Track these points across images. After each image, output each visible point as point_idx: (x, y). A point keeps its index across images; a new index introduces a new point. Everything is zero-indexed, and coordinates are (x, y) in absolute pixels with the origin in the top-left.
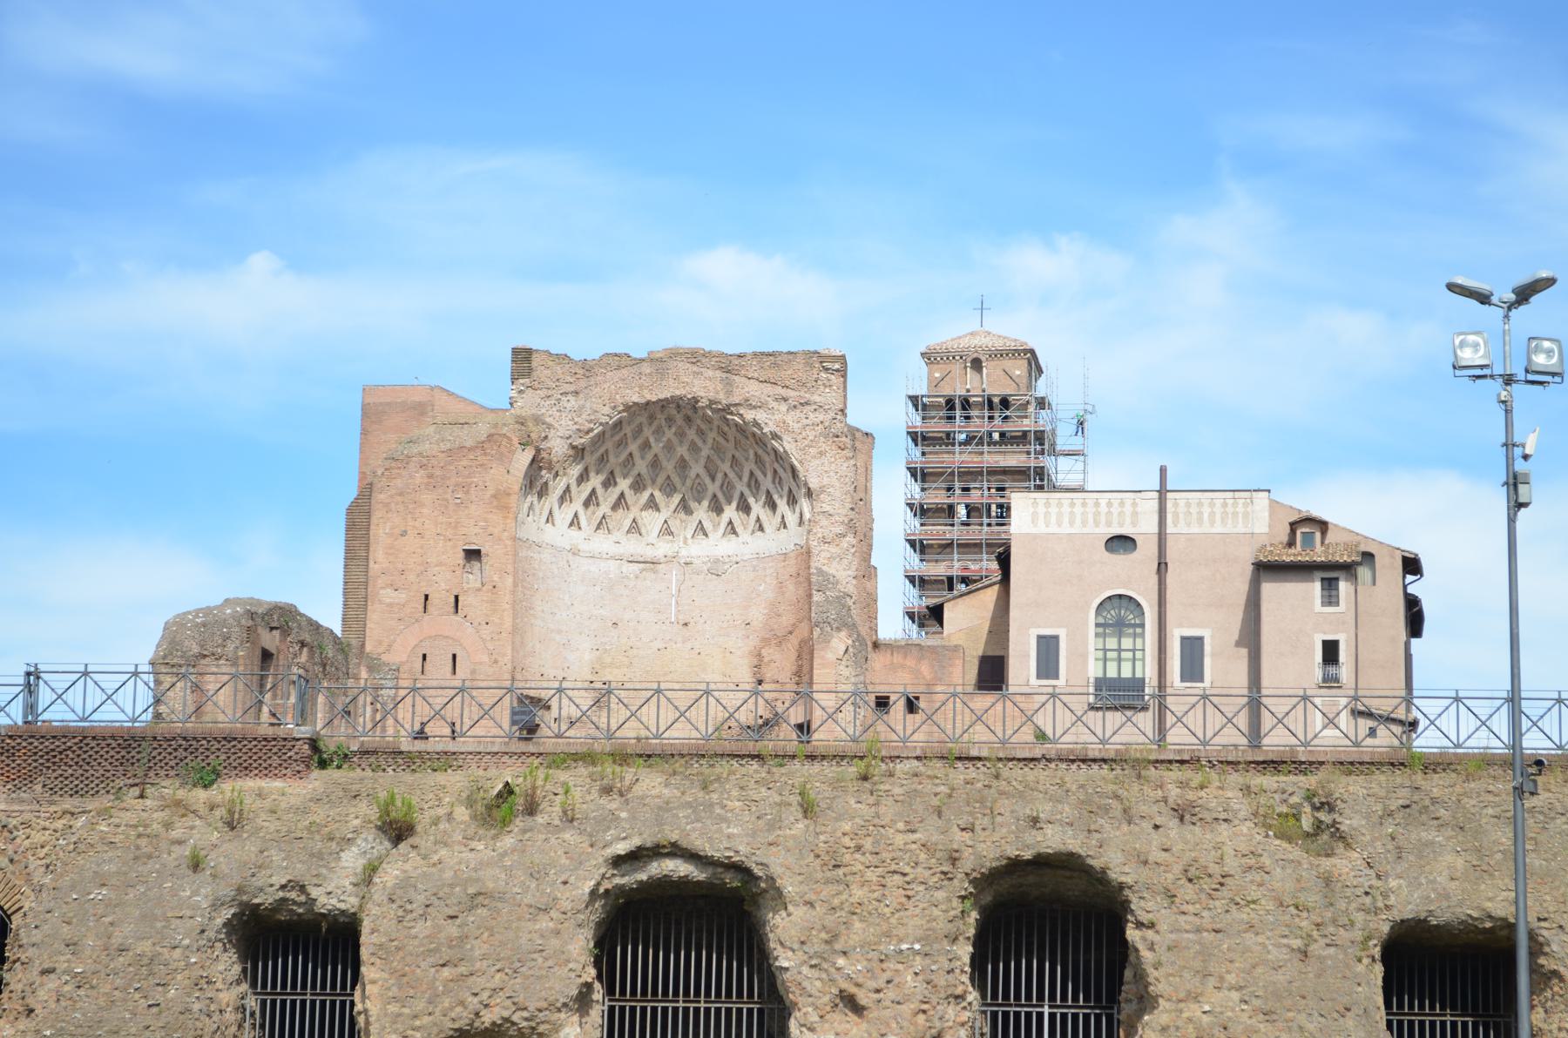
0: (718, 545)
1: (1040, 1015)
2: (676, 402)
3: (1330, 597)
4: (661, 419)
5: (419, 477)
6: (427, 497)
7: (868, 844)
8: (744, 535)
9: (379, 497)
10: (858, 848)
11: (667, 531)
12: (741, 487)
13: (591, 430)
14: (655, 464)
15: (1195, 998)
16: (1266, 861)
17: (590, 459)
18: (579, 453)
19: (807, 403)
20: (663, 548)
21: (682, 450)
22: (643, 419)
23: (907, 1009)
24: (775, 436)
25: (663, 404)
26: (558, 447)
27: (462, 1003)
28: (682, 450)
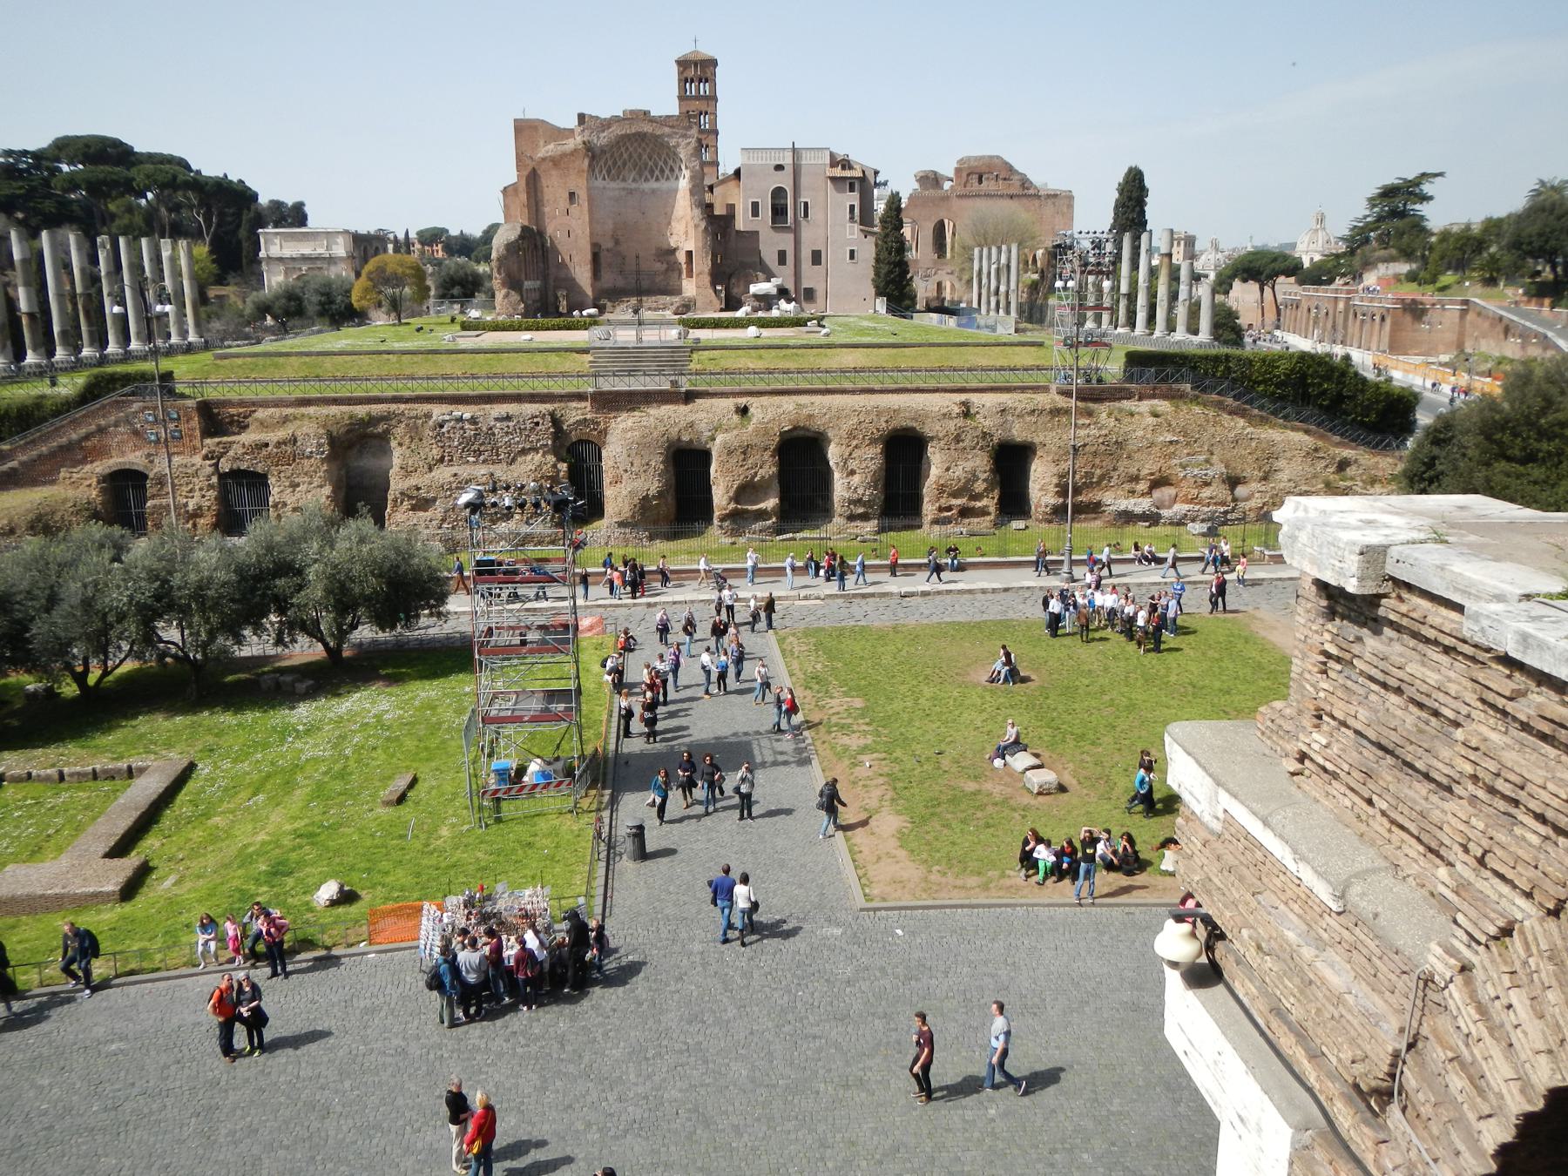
0: (653, 184)
6: (554, 172)
8: (663, 181)
11: (634, 180)
12: (661, 163)
14: (630, 156)
17: (608, 155)
20: (634, 186)
21: (640, 150)
25: (634, 135)
26: (598, 152)
28: (640, 150)
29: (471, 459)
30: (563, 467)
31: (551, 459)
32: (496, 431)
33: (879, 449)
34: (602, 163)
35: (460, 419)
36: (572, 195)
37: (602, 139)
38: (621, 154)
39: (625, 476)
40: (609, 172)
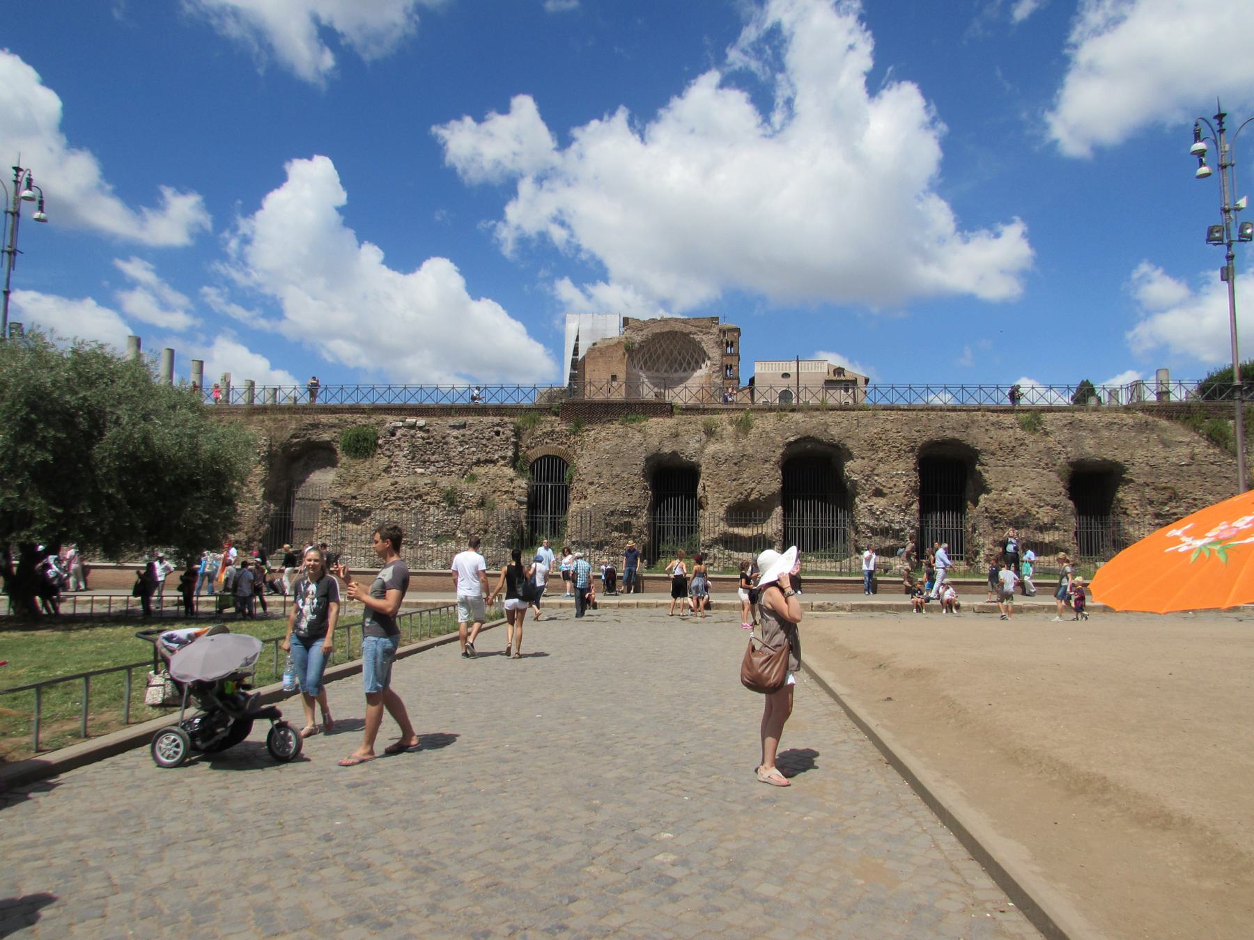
1: (936, 497)
2: (670, 332)
3: (846, 390)
4: (666, 337)
5: (598, 353)
6: (600, 360)
7: (884, 437)
9: (587, 360)
10: (881, 439)
13: (645, 342)
15: (1005, 490)
16: (1026, 442)
18: (641, 347)
19: (708, 333)
20: (665, 375)
21: (671, 347)
22: (661, 337)
23: (901, 494)
24: (699, 342)
27: (741, 494)
28: (671, 347)
29: (420, 470)
30: (523, 483)
31: (510, 472)
32: (451, 440)
33: (911, 462)
34: (640, 355)
35: (413, 427)
36: (614, 378)
37: (638, 338)
38: (656, 351)
39: (591, 490)
40: (645, 363)
